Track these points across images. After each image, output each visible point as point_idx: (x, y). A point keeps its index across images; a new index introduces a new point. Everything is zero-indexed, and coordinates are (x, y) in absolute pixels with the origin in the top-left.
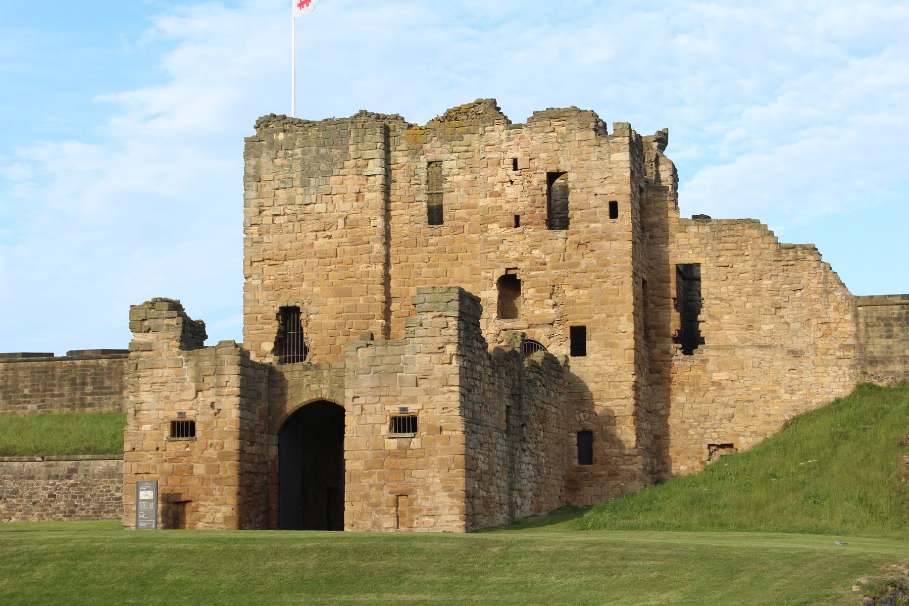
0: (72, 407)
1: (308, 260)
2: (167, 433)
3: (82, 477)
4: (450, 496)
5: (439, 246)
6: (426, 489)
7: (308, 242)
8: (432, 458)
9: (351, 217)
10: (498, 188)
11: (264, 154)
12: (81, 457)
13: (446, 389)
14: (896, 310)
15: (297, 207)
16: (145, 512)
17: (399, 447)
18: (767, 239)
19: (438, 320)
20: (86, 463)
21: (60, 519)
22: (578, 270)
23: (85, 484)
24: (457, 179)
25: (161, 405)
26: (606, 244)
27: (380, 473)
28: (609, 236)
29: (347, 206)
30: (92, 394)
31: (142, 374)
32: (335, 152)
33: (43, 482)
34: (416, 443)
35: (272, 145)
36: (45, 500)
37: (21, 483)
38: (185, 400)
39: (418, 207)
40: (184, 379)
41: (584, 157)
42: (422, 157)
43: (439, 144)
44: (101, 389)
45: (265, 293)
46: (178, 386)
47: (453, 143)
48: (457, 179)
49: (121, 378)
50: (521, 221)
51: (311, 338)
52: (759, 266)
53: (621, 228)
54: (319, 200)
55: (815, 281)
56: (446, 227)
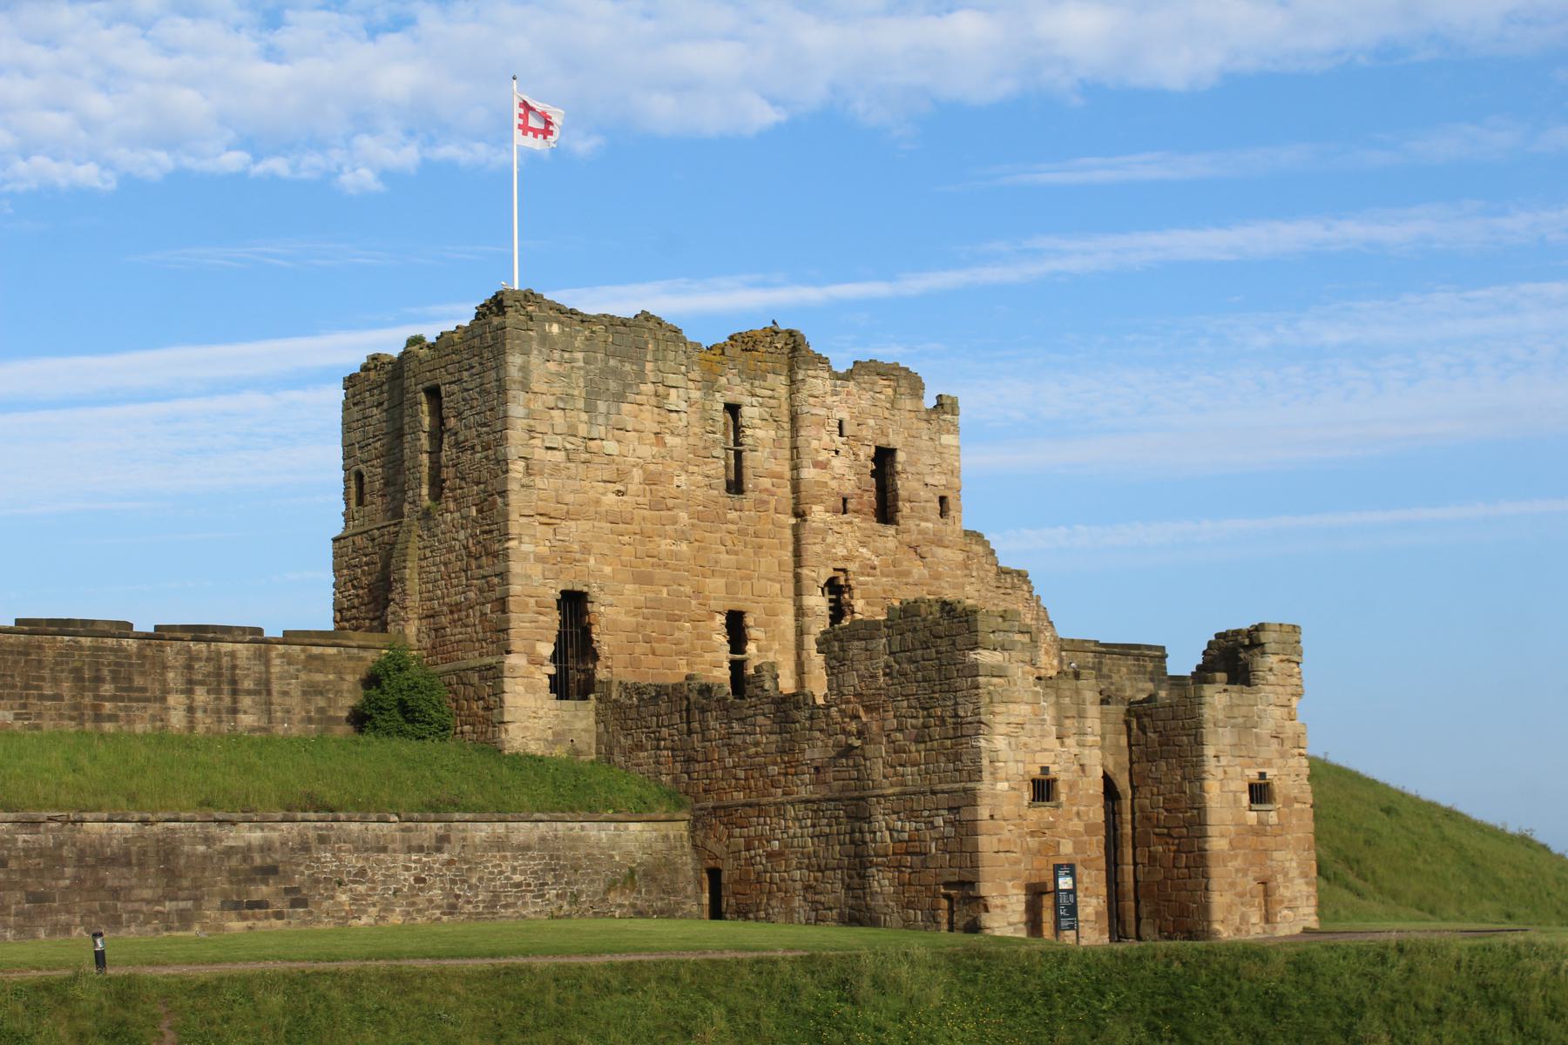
0: (80, 719)
2: (1027, 796)
3: (458, 849)
4: (1307, 884)
5: (742, 525)
6: (1286, 875)
7: (592, 494)
9: (652, 467)
12: (457, 816)
13: (1296, 751)
14: (1090, 658)
15: (578, 441)
17: (1260, 822)
20: (461, 826)
21: (439, 919)
24: (760, 433)
26: (940, 551)
29: (646, 451)
30: (113, 699)
32: (628, 367)
33: (401, 857)
34: (1273, 818)
35: (545, 339)
36: (411, 888)
37: (367, 859)
42: (718, 395)
43: (738, 380)
44: (127, 691)
45: (539, 567)
46: (1037, 730)
47: (757, 383)
48: (760, 433)
49: (162, 674)
50: (849, 506)
51: (604, 640)
53: (953, 532)
56: (750, 497)
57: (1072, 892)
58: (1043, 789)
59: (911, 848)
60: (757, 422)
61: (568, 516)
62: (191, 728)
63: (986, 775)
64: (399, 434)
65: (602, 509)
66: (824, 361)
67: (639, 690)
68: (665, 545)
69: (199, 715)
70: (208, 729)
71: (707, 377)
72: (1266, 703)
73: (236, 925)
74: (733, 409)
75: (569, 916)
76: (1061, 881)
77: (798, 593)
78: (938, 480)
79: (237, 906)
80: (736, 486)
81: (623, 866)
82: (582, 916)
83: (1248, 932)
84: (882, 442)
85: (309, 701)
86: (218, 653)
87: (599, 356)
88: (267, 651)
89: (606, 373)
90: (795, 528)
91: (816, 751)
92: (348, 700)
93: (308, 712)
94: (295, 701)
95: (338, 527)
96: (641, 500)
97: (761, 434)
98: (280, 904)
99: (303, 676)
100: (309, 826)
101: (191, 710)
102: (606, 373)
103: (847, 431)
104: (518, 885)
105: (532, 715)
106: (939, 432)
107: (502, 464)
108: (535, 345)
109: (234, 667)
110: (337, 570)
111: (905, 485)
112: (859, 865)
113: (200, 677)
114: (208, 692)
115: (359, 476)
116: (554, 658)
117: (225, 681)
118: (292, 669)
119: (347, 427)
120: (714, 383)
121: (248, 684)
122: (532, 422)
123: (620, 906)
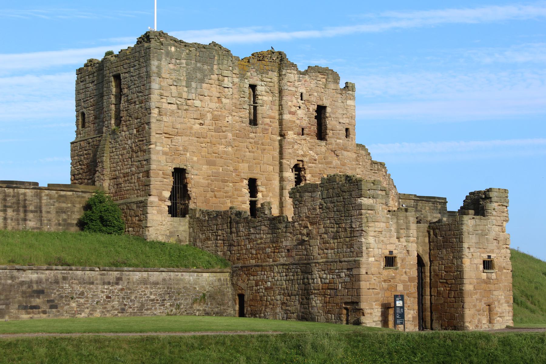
1: (190, 138)
2: (383, 264)
3: (126, 284)
4: (508, 306)
5: (256, 140)
6: (499, 302)
7: (189, 124)
8: (501, 285)
9: (216, 113)
10: (293, 109)
11: (164, 59)
12: (125, 269)
13: (505, 246)
16: (399, 314)
17: (488, 278)
18: (368, 156)
19: (500, 207)
20: (127, 273)
21: (117, 315)
22: (332, 166)
23: (129, 289)
24: (265, 98)
25: (380, 246)
26: (345, 153)
27: (480, 292)
28: (346, 148)
29: (213, 105)
31: (370, 225)
32: (206, 67)
33: (100, 287)
34: (494, 276)
35: (168, 54)
36: (104, 301)
37: (85, 287)
38: (392, 243)
39: (244, 113)
40: (391, 230)
41: (334, 99)
42: (246, 80)
45: (164, 157)
47: (264, 75)
50: (305, 132)
51: (193, 191)
52: (365, 172)
53: (352, 144)
54: (197, 98)
55: (385, 183)
56: (260, 127)
57: (402, 307)
58: (390, 261)
59: (330, 287)
60: (264, 93)
61: (177, 134)
62: (5, 226)
63: (364, 254)
64: (101, 96)
65: (193, 131)
66: (294, 66)
67: (209, 213)
68: (221, 148)
69: (9, 221)
70: (13, 228)
71: (241, 72)
72: (491, 224)
73: (25, 316)
74: (253, 87)
75: (175, 314)
76: (397, 302)
77: (281, 171)
78: (345, 121)
79: (25, 308)
80: (254, 122)
81: (199, 292)
82: (182, 314)
83: (481, 328)
84: (320, 103)
85: (59, 216)
86: (18, 193)
87: (193, 62)
88: (40, 193)
89: (196, 69)
90: (280, 142)
91: (288, 242)
92: (77, 216)
93: (59, 221)
94: (53, 216)
95: (73, 137)
96: (211, 127)
97: (265, 99)
98: (45, 307)
99: (57, 205)
100: (58, 272)
101: (5, 219)
102: (196, 69)
103: (304, 98)
104: (153, 300)
105: (160, 224)
106: (346, 99)
107: (148, 110)
108: (164, 56)
109: (25, 200)
110: (72, 157)
111: (330, 123)
112: (306, 294)
113: (10, 204)
114: (13, 211)
115: (83, 114)
116: (170, 198)
117: (21, 206)
118: (52, 201)
119: (78, 92)
120: (244, 75)
121: (31, 208)
122: (162, 91)
123: (198, 310)
